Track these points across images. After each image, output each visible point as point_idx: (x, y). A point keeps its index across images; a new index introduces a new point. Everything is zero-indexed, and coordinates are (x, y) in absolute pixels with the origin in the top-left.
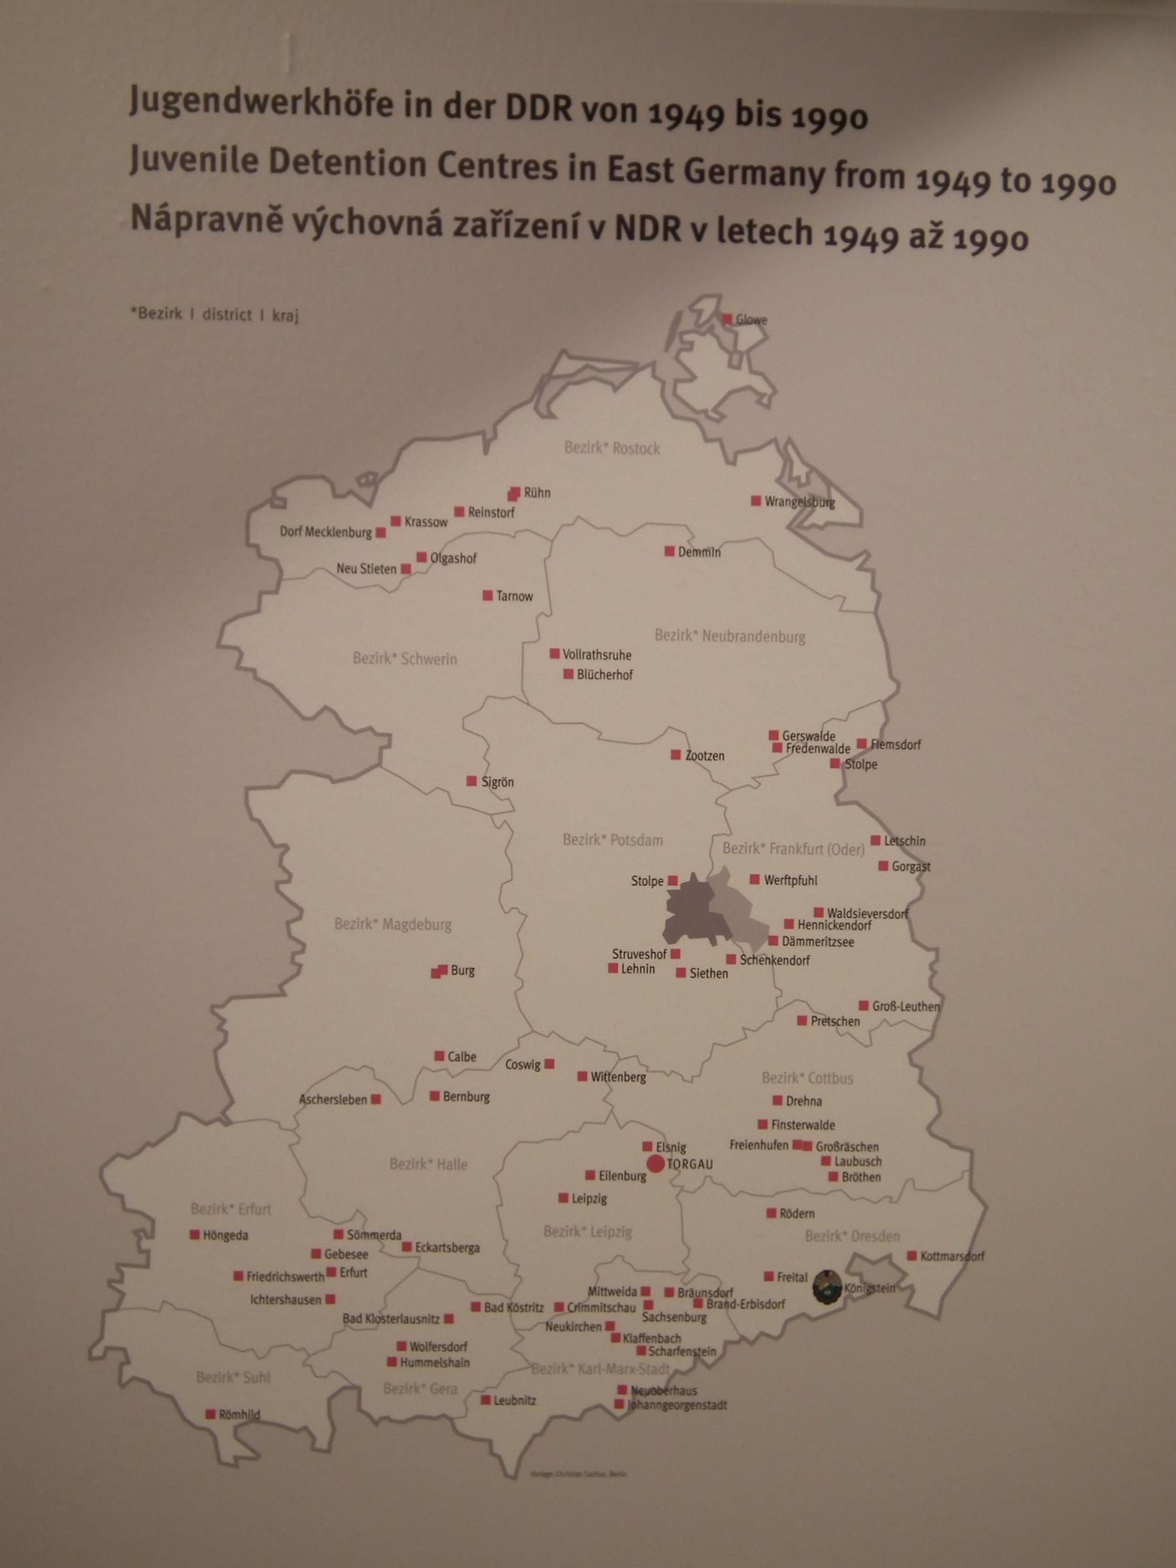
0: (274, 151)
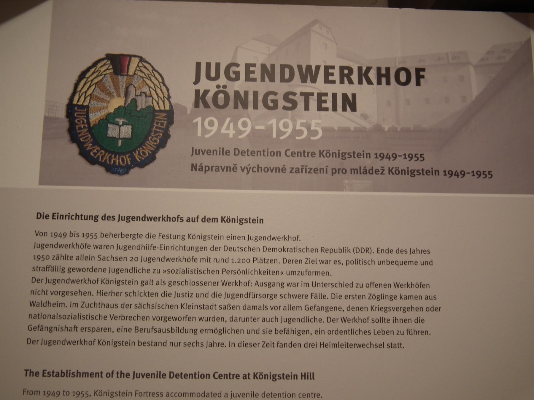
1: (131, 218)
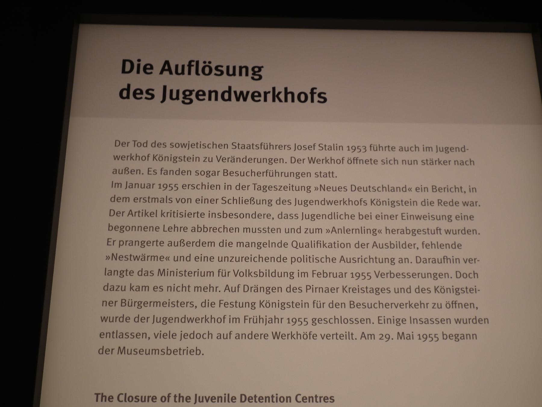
0: (241, 395)
1: (194, 93)
